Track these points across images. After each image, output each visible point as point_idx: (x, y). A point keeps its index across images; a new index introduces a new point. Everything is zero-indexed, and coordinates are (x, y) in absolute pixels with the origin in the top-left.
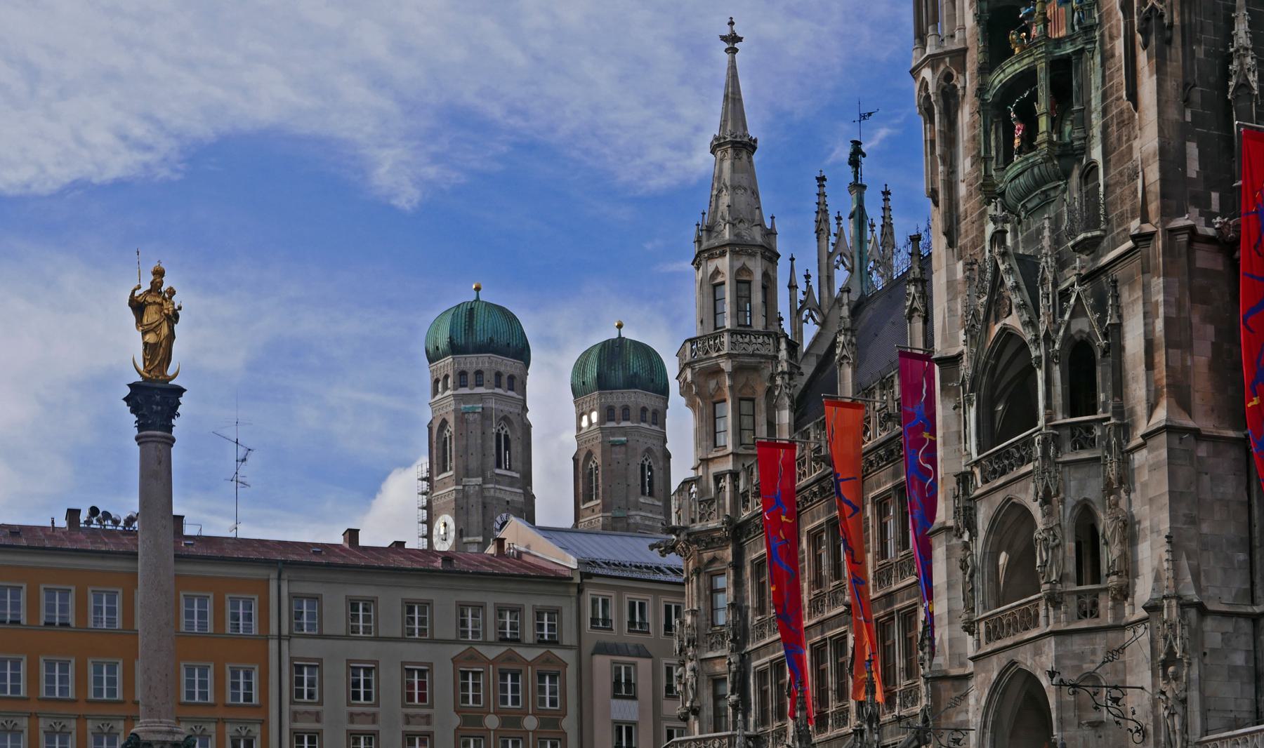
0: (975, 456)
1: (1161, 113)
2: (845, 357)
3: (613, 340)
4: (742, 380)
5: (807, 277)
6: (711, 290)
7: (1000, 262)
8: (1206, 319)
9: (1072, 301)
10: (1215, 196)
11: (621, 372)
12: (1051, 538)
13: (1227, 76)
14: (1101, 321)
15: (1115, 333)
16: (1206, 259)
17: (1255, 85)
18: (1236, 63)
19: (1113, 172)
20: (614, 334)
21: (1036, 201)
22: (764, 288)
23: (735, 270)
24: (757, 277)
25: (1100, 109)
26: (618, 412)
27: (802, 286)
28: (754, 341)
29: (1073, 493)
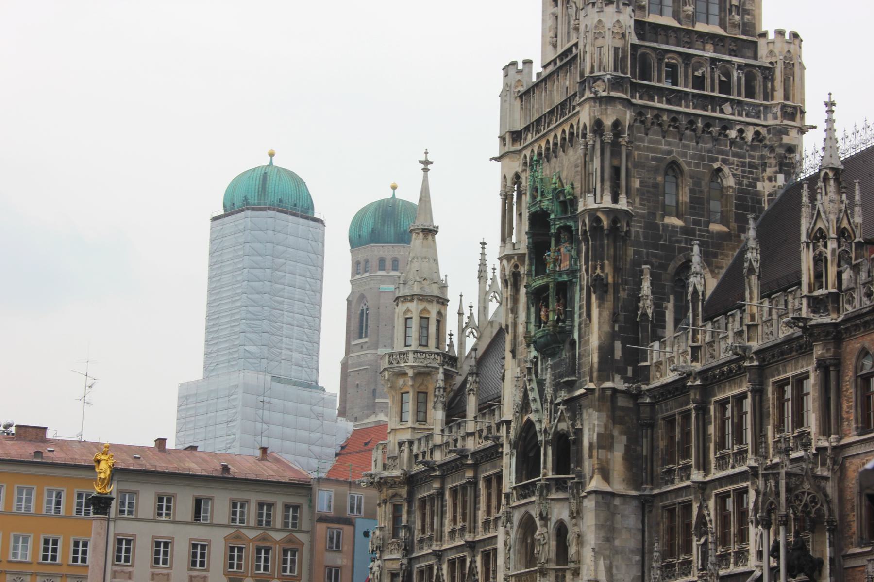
0: (514, 485)
1: (599, 329)
2: (471, 390)
3: (388, 200)
4: (419, 380)
5: (471, 307)
6: (404, 321)
7: (528, 384)
8: (622, 433)
9: (559, 413)
10: (630, 369)
11: (392, 228)
12: (542, 539)
13: (638, 309)
14: (573, 425)
15: (579, 432)
16: (622, 402)
17: (650, 315)
18: (642, 302)
19: (582, 349)
20: (388, 195)
21: (549, 352)
22: (438, 321)
23: (419, 310)
24: (433, 316)
25: (578, 313)
26: (388, 263)
27: (467, 313)
28: (428, 357)
29: (555, 516)
